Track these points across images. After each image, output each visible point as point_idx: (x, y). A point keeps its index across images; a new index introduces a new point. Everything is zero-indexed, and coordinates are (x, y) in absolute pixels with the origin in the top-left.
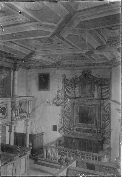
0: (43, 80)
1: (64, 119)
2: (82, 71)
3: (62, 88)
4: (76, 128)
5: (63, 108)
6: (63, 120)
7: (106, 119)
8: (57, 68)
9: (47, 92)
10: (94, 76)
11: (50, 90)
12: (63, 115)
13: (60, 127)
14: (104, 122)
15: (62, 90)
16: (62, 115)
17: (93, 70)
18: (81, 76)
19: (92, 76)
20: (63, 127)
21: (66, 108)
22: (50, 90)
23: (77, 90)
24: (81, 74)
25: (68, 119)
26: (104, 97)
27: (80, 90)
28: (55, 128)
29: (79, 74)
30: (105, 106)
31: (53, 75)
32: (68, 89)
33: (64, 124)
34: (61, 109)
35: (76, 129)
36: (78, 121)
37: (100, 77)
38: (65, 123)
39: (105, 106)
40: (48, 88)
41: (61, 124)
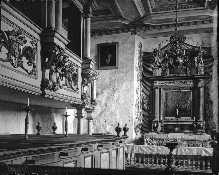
2: (169, 38)
3: (139, 65)
9: (113, 70)
12: (139, 107)
17: (187, 36)
18: (168, 45)
20: (139, 124)
24: (168, 43)
25: (146, 114)
31: (123, 43)
32: (146, 67)
33: (140, 120)
34: (137, 96)
38: (141, 119)
41: (137, 120)
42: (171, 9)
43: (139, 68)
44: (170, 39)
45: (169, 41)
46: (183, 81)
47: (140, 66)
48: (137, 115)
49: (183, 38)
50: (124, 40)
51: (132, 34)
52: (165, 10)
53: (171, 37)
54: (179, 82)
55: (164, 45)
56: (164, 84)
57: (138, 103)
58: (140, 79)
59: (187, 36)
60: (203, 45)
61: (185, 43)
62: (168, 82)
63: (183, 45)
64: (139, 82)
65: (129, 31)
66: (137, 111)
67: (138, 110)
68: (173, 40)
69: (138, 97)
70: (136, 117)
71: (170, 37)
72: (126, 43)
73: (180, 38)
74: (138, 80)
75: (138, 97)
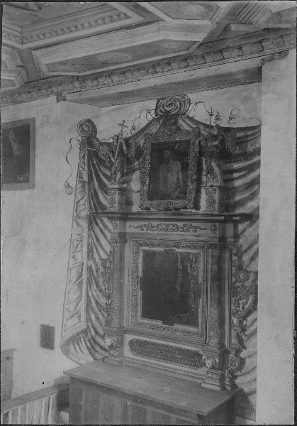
0: (15, 146)
1: (88, 304)
2: (152, 104)
3: (80, 176)
4: (128, 338)
5: (85, 255)
6: (83, 305)
7: (246, 307)
8: (53, 98)
9: (27, 192)
10: (198, 123)
11: (33, 187)
13: (69, 334)
14: (235, 320)
15: (79, 186)
16: (81, 283)
17: (193, 97)
19: (191, 119)
20: (85, 332)
21: (99, 255)
22: (33, 187)
23: (135, 185)
24: (150, 118)
26: (241, 210)
27: (143, 183)
28: (47, 338)
29: (143, 114)
30: (244, 248)
33: (88, 319)
34: (72, 260)
35: (131, 343)
36: (139, 314)
37: (224, 124)
39: (244, 248)
40: (27, 180)
42: (60, 32)
43: (83, 187)
44: (154, 107)
45: (153, 112)
46: (180, 224)
47: (86, 179)
48: (72, 308)
49: (184, 101)
50: (44, 116)
51: (58, 101)
52: (47, 35)
53: (158, 102)
54: (171, 227)
55: (143, 122)
56: (138, 230)
57: (80, 275)
58: (85, 213)
59: (193, 97)
60: (232, 121)
61: (188, 117)
62: (147, 223)
63: (184, 124)
64: (84, 224)
65: (52, 92)
66: (73, 296)
67: (78, 294)
68: (161, 108)
69: (79, 259)
70: (67, 315)
71: (156, 101)
72: (48, 122)
73: (178, 104)
74: (77, 217)
75: (79, 259)
